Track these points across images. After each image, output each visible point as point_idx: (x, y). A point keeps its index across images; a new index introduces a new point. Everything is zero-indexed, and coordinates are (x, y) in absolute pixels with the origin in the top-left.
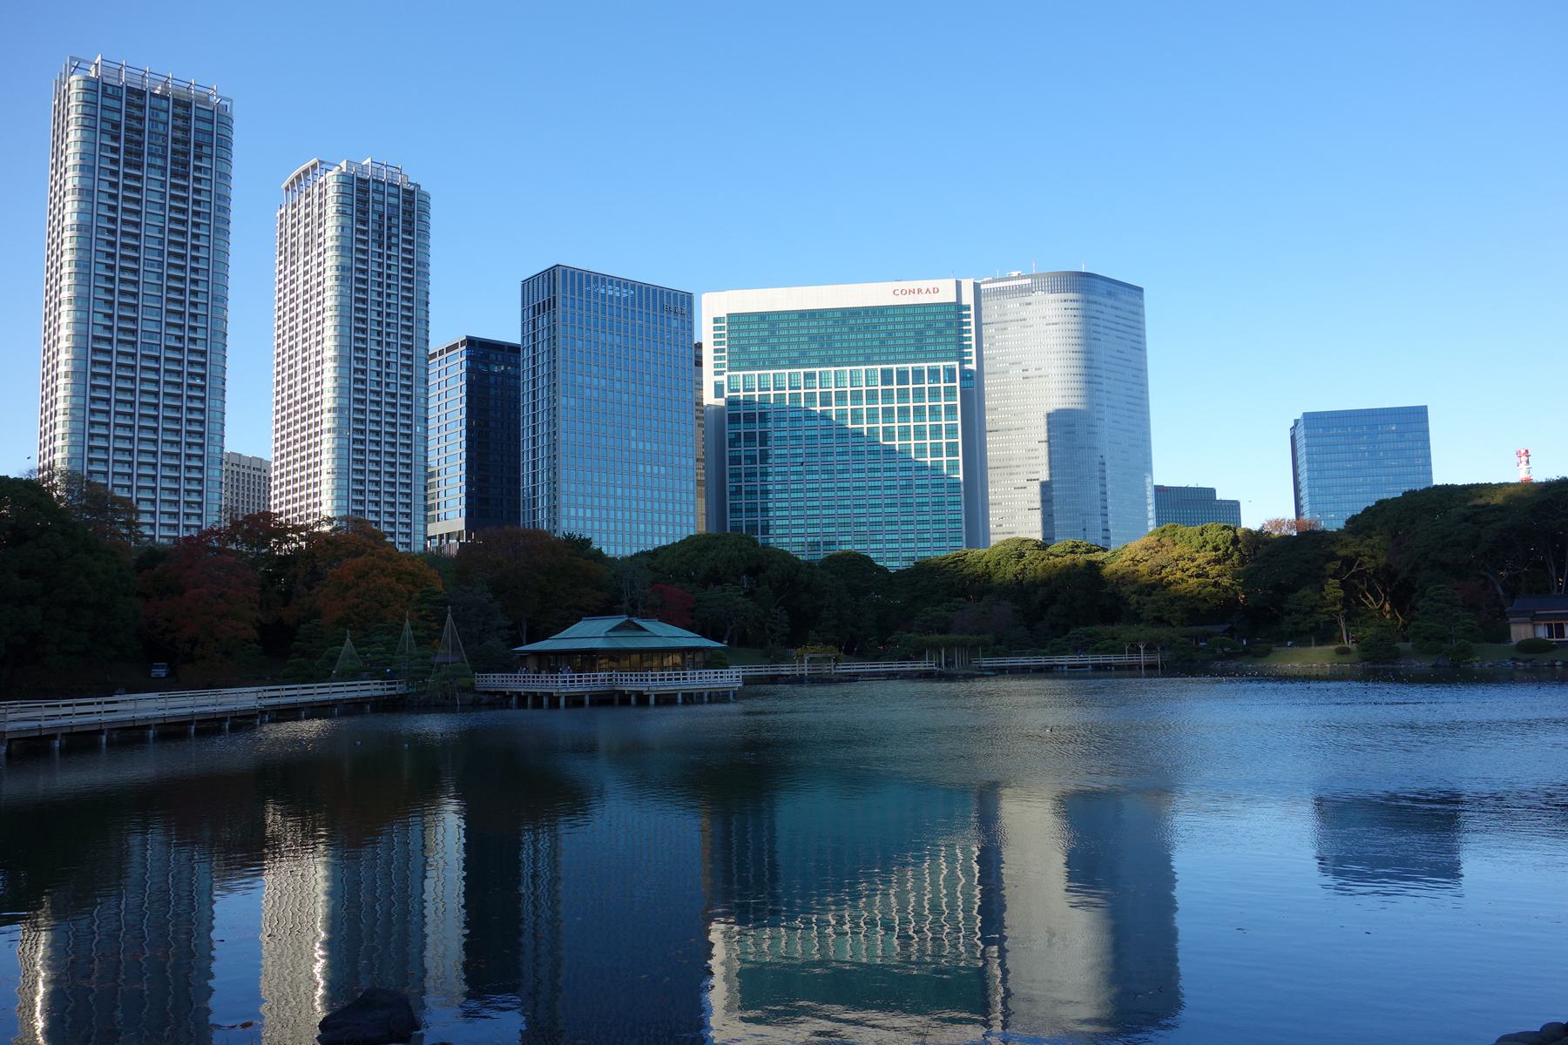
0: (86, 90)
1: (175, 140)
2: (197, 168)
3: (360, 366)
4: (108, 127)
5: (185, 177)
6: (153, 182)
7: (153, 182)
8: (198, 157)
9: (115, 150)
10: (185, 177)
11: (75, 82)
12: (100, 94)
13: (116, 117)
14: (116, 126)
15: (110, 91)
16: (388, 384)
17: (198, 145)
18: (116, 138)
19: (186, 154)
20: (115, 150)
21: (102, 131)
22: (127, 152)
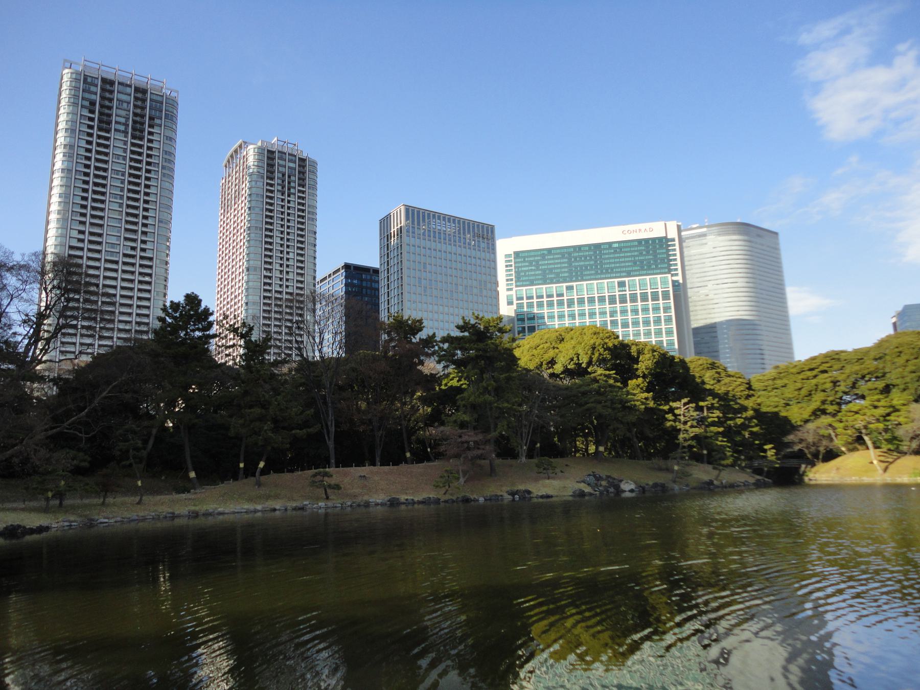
0: (77, 80)
1: (135, 114)
2: (150, 133)
3: (269, 274)
4: (87, 103)
5: (141, 139)
6: (119, 143)
7: (119, 143)
8: (151, 126)
9: (91, 119)
10: (141, 139)
11: (67, 74)
12: (84, 82)
13: (93, 97)
14: (93, 103)
15: (89, 80)
16: (287, 287)
17: (151, 118)
18: (92, 112)
19: (143, 124)
20: (91, 119)
21: (82, 106)
22: (100, 121)
